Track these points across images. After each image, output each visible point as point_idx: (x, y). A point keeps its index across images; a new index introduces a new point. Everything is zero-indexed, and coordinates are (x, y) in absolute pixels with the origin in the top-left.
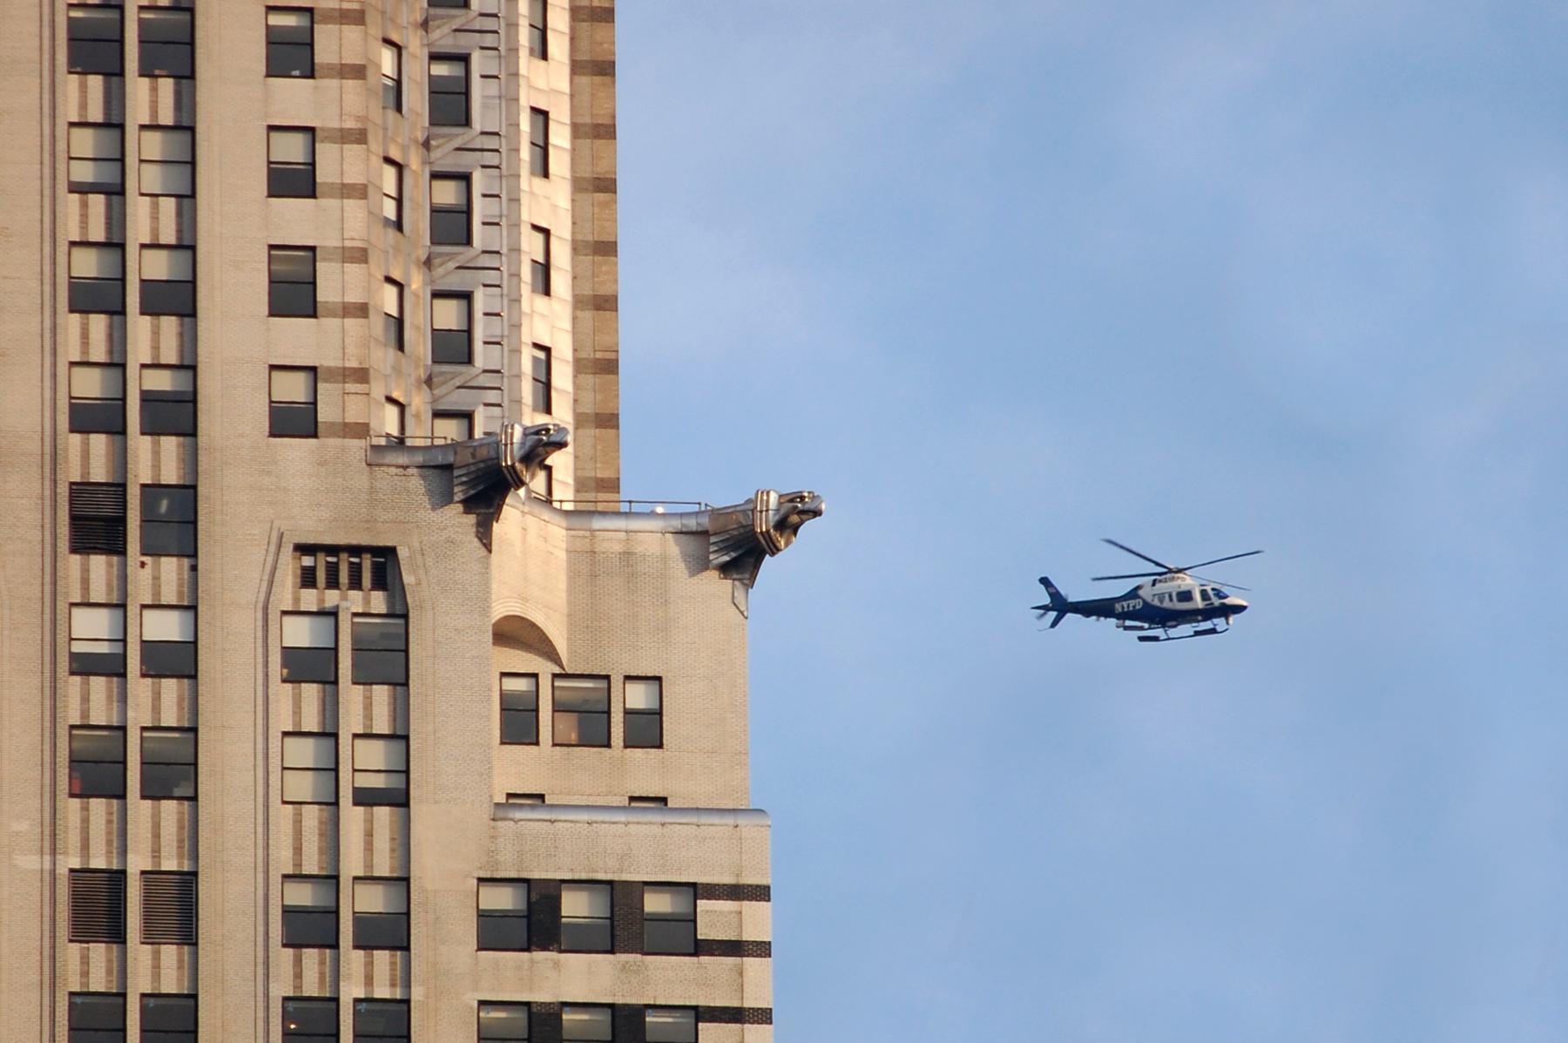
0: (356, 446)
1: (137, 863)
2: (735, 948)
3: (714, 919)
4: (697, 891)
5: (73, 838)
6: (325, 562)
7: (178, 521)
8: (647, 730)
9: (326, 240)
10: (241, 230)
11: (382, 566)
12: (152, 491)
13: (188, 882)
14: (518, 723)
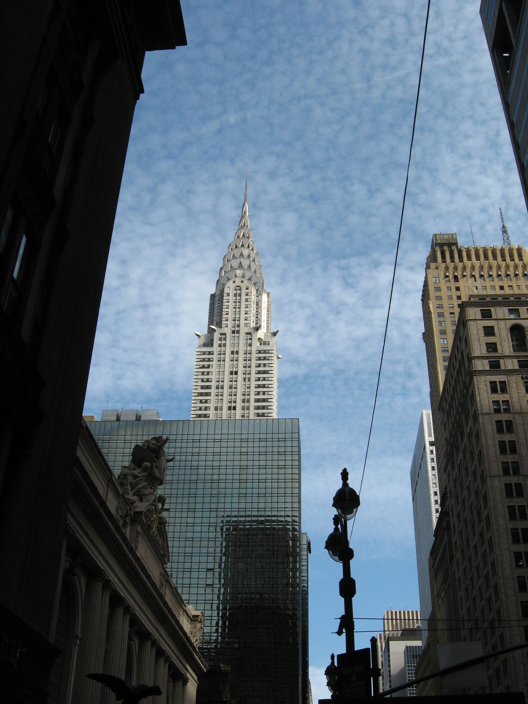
6: (247, 334)
7: (238, 332)
8: (268, 344)
10: (243, 316)
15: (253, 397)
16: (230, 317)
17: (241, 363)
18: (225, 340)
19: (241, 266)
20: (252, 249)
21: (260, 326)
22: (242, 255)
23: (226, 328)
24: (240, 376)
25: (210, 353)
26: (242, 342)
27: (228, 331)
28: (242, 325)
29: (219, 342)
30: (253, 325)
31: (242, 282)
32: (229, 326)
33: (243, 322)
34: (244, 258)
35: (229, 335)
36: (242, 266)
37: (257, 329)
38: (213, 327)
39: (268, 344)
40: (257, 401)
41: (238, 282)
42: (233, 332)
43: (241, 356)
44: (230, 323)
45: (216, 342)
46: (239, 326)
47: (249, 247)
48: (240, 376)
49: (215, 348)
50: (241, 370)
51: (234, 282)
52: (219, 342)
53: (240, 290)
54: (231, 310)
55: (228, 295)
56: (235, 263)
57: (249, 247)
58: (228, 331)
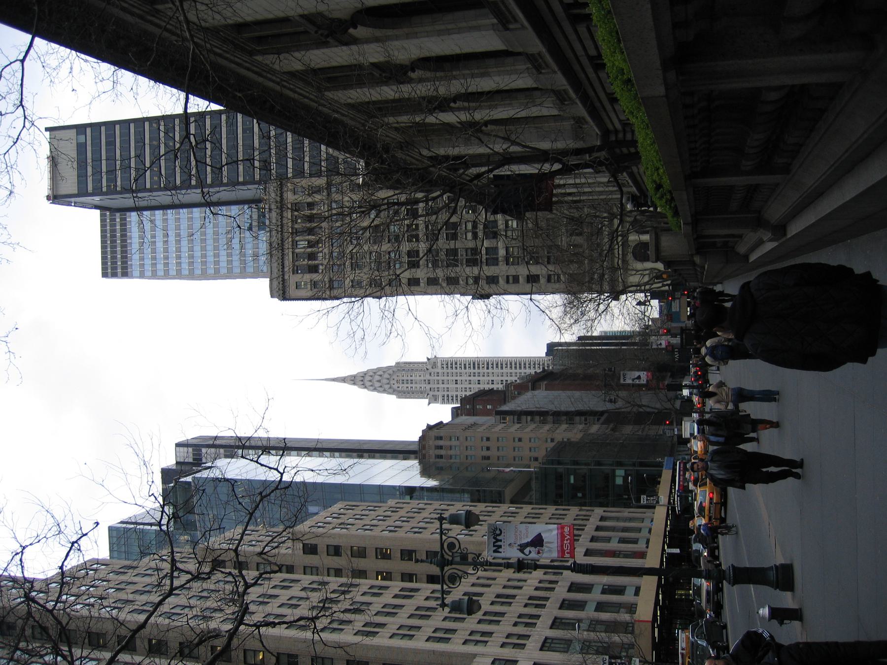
15: (472, 371)
17: (450, 378)
24: (459, 378)
27: (428, 387)
35: (431, 386)
40: (474, 368)
41: (395, 382)
43: (445, 378)
44: (423, 386)
48: (459, 378)
50: (455, 378)
54: (414, 385)
56: (377, 385)
58: (428, 387)
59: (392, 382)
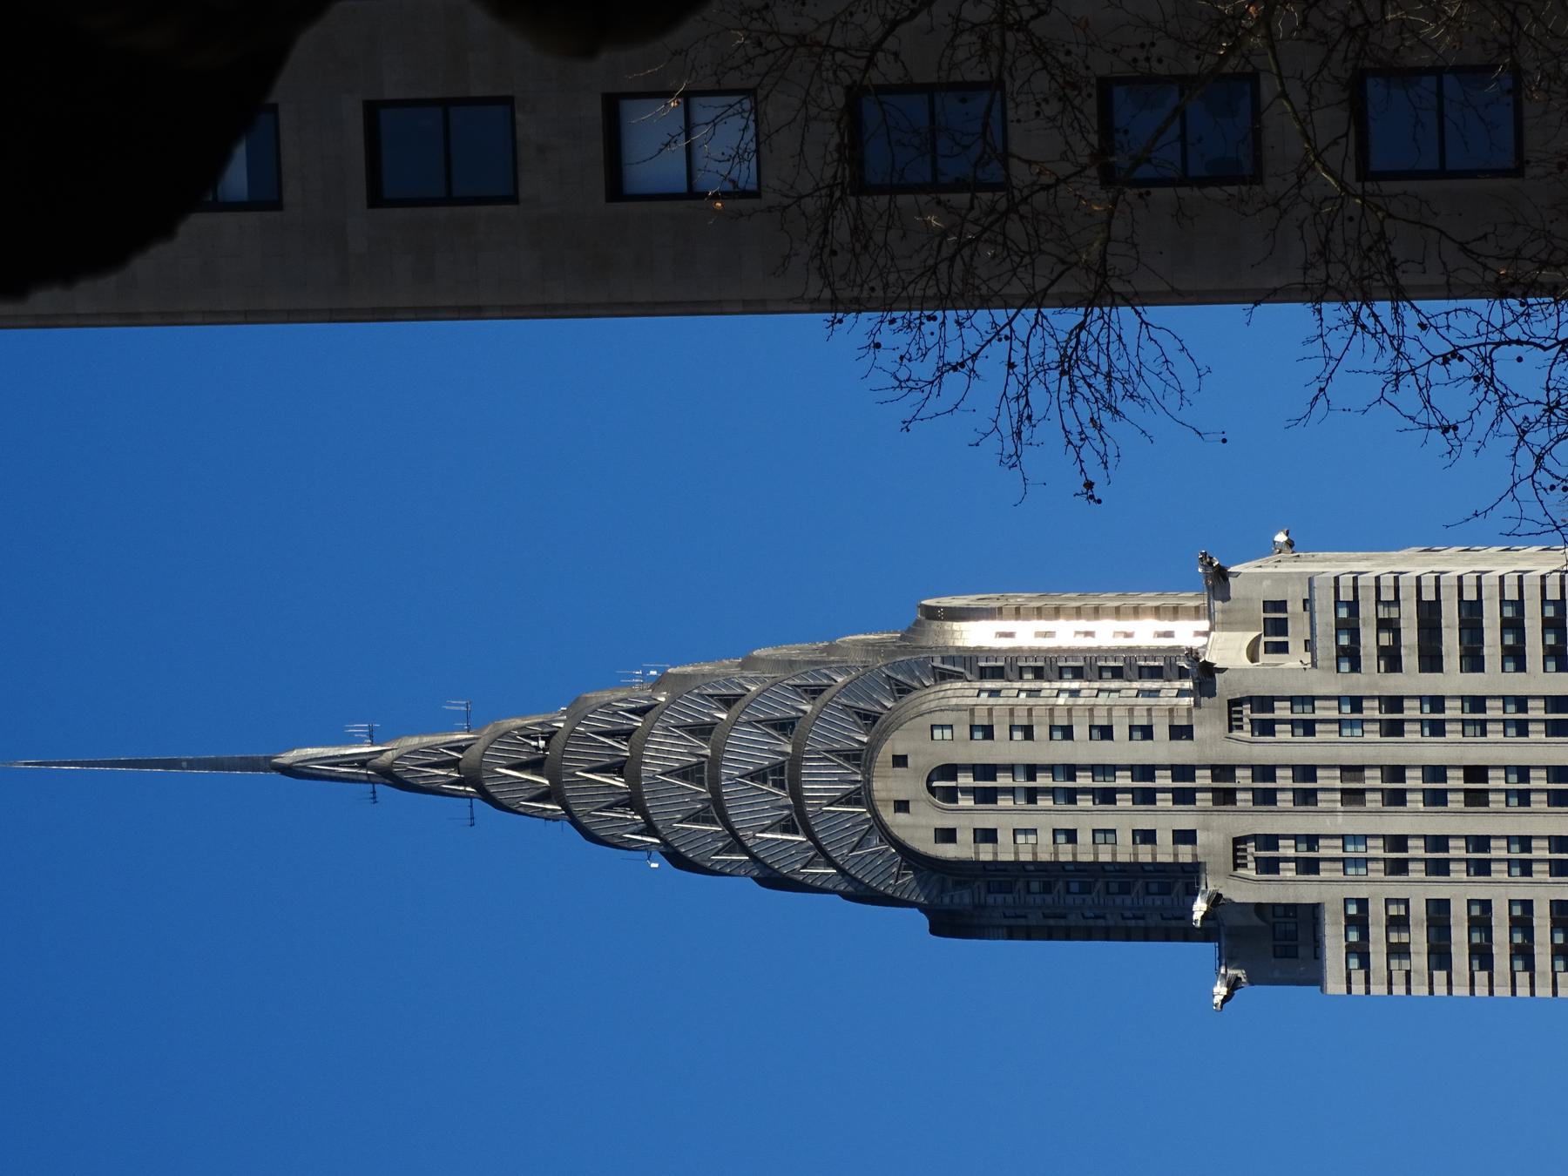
0: (1195, 712)
1: (1338, 784)
2: (1355, 589)
3: (1347, 595)
4: (1337, 601)
5: (1331, 805)
6: (1233, 724)
7: (1223, 771)
9: (1127, 722)
11: (1233, 703)
12: (1214, 779)
13: (1343, 768)
14: (1282, 648)
16: (1125, 818)
18: (1270, 841)
19: (784, 774)
20: (641, 712)
21: (1192, 655)
22: (685, 773)
23: (1201, 837)
25: (1358, 922)
26: (1285, 748)
27: (1216, 831)
28: (1183, 752)
29: (1288, 871)
30: (1173, 695)
31: (900, 761)
32: (1185, 822)
33: (1161, 750)
34: (715, 762)
36: (777, 769)
37: (1205, 675)
38: (1200, 907)
39: (1280, 606)
41: (908, 785)
42: (1225, 797)
44: (1165, 819)
45: (1288, 888)
46: (1183, 772)
47: (627, 735)
49: (1328, 892)
51: (902, 806)
52: (1288, 871)
53: (950, 771)
55: (988, 836)
57: (627, 735)
59: (888, 785)
